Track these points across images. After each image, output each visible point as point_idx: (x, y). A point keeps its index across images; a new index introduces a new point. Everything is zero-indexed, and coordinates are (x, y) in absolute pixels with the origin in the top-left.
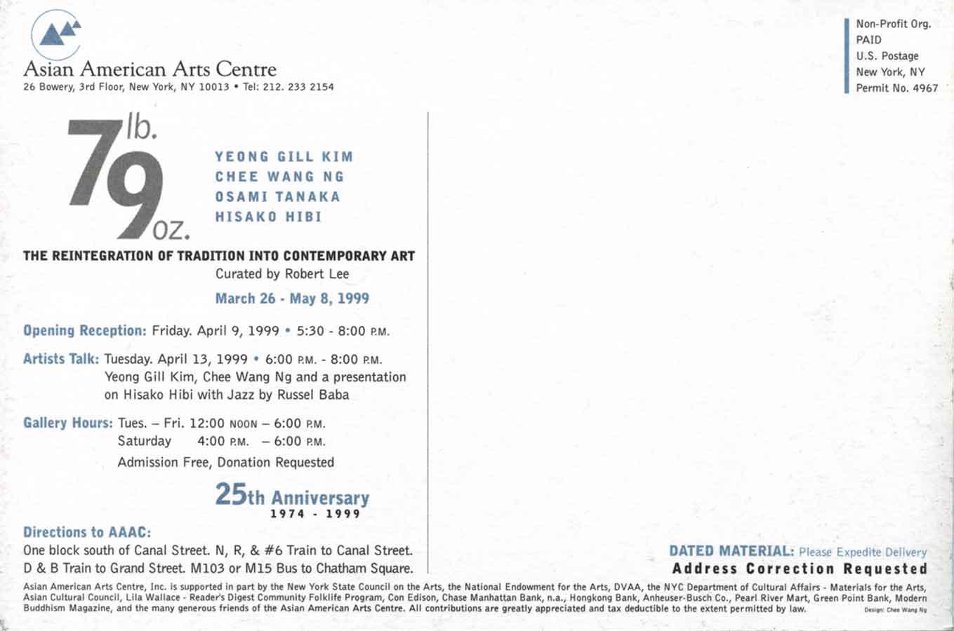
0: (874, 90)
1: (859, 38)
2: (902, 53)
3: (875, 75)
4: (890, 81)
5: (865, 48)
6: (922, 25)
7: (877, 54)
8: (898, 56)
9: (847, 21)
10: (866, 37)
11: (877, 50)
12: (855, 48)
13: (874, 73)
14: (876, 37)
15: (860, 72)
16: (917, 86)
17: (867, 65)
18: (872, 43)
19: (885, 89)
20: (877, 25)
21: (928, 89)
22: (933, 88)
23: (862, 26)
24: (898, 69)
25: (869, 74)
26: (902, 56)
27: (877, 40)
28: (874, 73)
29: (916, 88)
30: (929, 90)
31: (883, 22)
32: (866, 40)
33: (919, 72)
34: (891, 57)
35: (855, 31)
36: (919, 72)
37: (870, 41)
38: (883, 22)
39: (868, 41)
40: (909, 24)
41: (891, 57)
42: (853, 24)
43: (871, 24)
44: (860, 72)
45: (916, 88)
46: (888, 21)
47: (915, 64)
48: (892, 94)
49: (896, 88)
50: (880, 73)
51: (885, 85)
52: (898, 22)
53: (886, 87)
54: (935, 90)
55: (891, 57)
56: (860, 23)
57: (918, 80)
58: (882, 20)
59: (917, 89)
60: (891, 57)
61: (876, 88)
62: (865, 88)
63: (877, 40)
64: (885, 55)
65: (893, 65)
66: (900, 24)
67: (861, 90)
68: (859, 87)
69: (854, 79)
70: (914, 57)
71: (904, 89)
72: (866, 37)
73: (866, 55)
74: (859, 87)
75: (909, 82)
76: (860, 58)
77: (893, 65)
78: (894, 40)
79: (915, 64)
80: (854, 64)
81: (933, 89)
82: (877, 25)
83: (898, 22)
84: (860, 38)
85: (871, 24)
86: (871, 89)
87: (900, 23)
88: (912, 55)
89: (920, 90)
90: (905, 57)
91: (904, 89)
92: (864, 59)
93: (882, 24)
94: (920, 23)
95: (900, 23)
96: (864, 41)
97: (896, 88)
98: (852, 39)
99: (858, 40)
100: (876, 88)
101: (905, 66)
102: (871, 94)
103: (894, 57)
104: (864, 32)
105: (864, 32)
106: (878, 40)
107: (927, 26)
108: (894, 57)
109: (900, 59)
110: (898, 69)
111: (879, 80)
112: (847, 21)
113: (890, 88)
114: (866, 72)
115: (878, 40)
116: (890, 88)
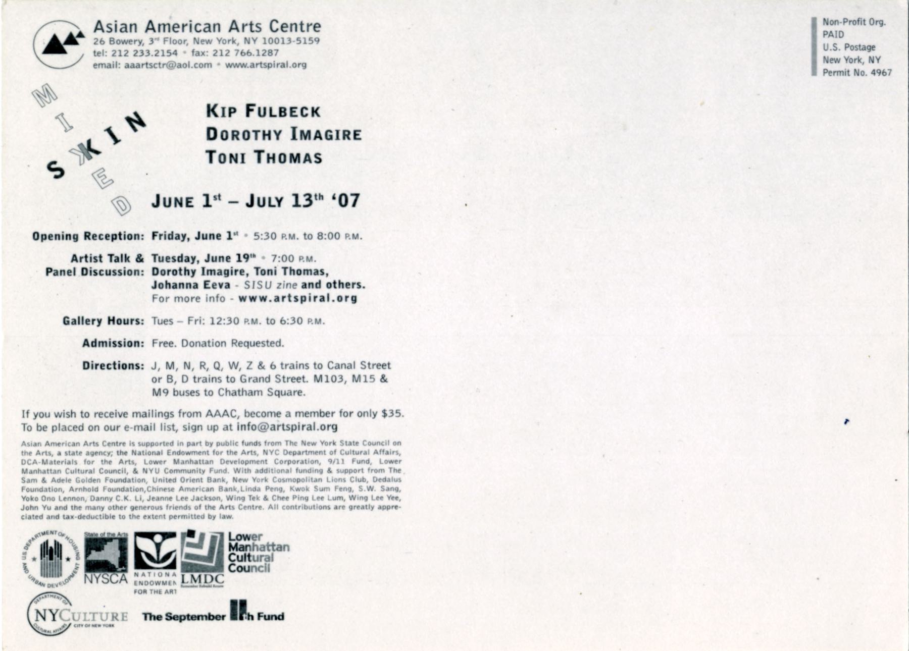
0: (837, 75)
1: (825, 33)
2: (862, 45)
3: (839, 62)
4: (852, 67)
5: (830, 41)
6: (878, 23)
7: (841, 46)
8: (858, 47)
9: (814, 20)
10: (831, 32)
11: (841, 43)
12: (821, 40)
13: (837, 61)
14: (840, 32)
15: (826, 60)
16: (874, 70)
17: (832, 54)
18: (836, 37)
19: (847, 73)
20: (841, 23)
21: (882, 73)
22: (888, 72)
23: (827, 24)
24: (859, 57)
25: (834, 61)
26: (861, 47)
27: (841, 34)
28: (837, 61)
29: (873, 73)
30: (884, 74)
31: (845, 21)
32: (831, 34)
33: (876, 61)
34: (853, 48)
35: (821, 28)
36: (876, 61)
37: (834, 35)
38: (845, 21)
39: (833, 36)
40: (867, 22)
41: (852, 48)
42: (820, 22)
43: (835, 22)
44: (826, 60)
45: (873, 73)
46: (849, 19)
47: (872, 54)
48: (852, 77)
49: (857, 72)
50: (843, 61)
51: (847, 70)
52: (858, 21)
53: (848, 71)
54: (889, 75)
55: (852, 48)
56: (826, 22)
57: (876, 66)
58: (844, 19)
59: (874, 74)
60: (853, 48)
61: (840, 73)
62: (830, 72)
63: (841, 34)
64: (847, 46)
65: (854, 54)
66: (860, 22)
67: (827, 75)
68: (826, 71)
69: (821, 66)
70: (872, 48)
71: (863, 74)
72: (831, 32)
73: (831, 47)
74: (826, 71)
75: (868, 68)
76: (826, 48)
77: (854, 54)
78: (855, 35)
79: (872, 54)
80: (821, 54)
81: (888, 74)
82: (841, 23)
83: (858, 21)
84: (826, 33)
85: (835, 22)
86: (836, 74)
87: (859, 21)
88: (870, 46)
89: (877, 74)
90: (864, 48)
91: (863, 74)
92: (829, 50)
93: (844, 22)
94: (877, 22)
95: (859, 21)
96: (829, 36)
97: (857, 72)
98: (820, 34)
99: (824, 35)
100: (840, 73)
101: (864, 55)
102: (835, 78)
103: (855, 48)
104: (829, 28)
105: (829, 28)
106: (841, 35)
107: (882, 24)
108: (855, 48)
109: (860, 50)
110: (859, 57)
111: (842, 66)
112: (814, 20)
113: (852, 73)
114: (832, 59)
115: (841, 35)
116: (852, 73)
